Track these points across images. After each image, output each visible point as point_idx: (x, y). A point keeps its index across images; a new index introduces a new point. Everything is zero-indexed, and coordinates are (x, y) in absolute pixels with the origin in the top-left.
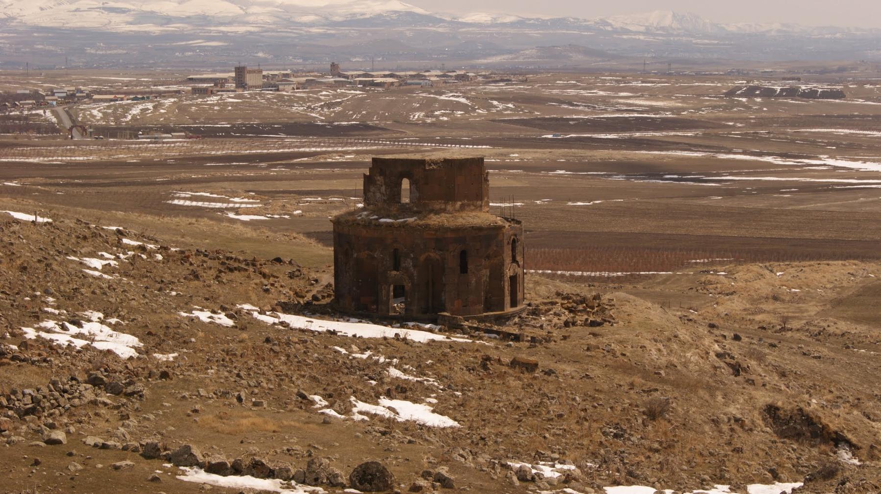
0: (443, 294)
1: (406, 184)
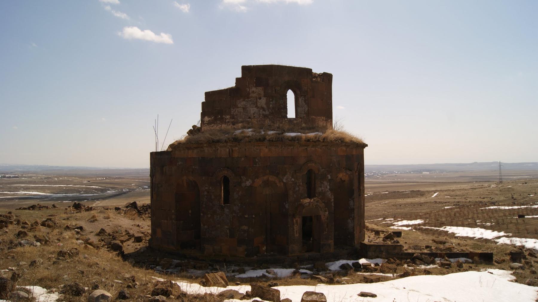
0: (349, 221)
1: (290, 96)
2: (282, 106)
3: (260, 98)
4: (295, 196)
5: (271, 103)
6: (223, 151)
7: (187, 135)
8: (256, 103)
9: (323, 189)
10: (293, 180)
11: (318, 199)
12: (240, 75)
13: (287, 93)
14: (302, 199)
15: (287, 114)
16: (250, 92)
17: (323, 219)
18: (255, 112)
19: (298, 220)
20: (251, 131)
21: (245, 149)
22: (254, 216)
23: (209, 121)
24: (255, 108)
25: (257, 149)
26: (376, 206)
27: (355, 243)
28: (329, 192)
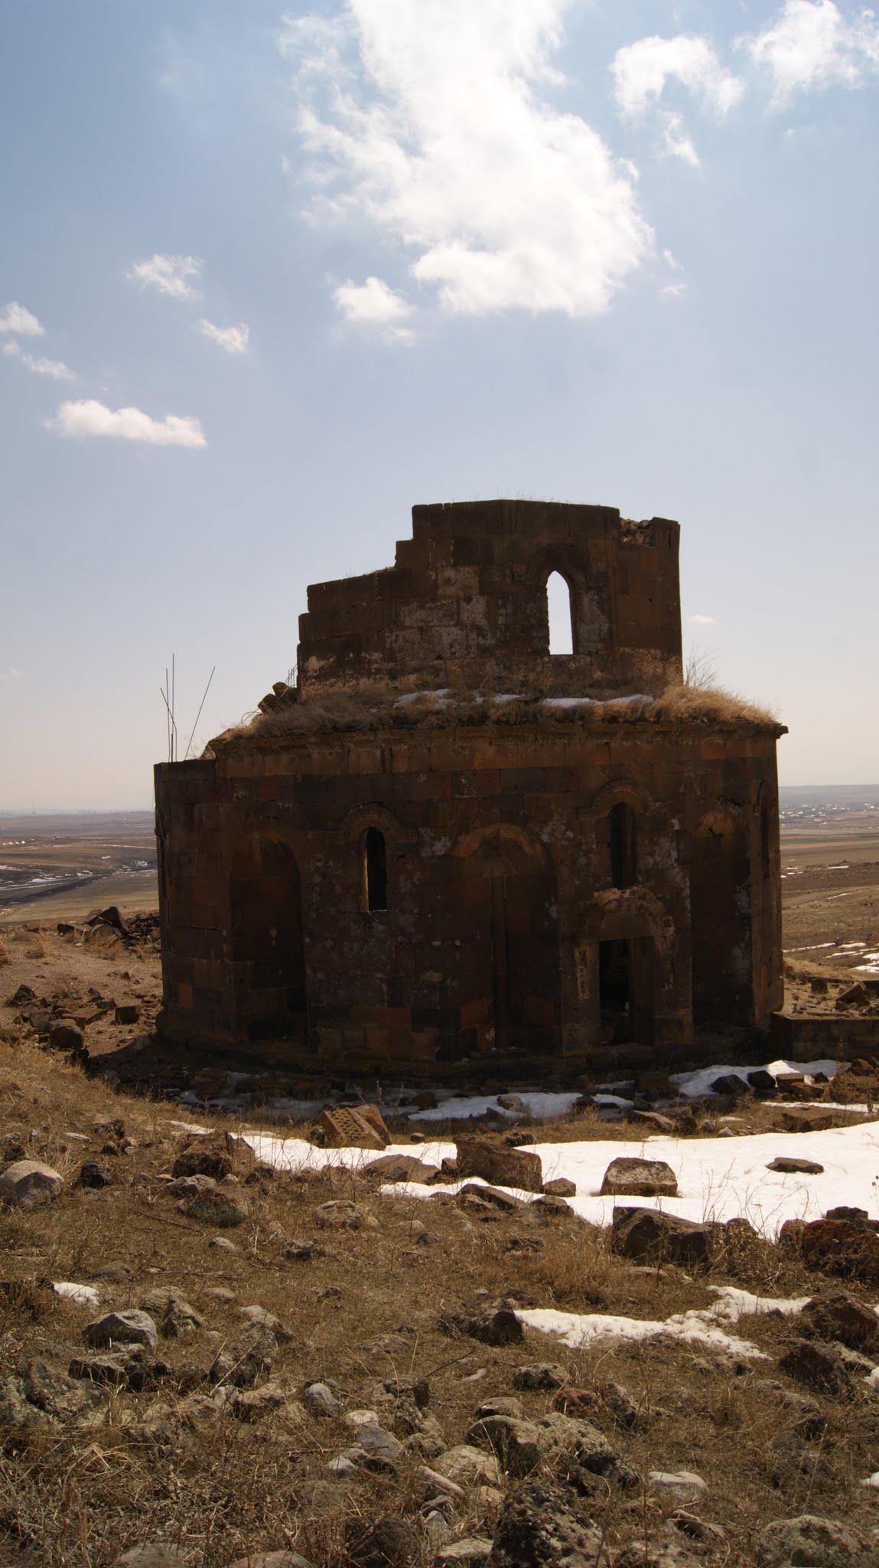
0: (737, 952)
1: (557, 588)
2: (533, 621)
3: (469, 600)
4: (577, 882)
5: (502, 611)
6: (364, 757)
7: (260, 711)
8: (459, 614)
9: (658, 859)
10: (570, 834)
11: (643, 890)
12: (408, 534)
13: (546, 583)
14: (597, 890)
15: (548, 642)
16: (440, 581)
17: (660, 945)
18: (455, 640)
19: (588, 951)
20: (446, 696)
21: (429, 750)
22: (458, 943)
23: (321, 668)
24: (455, 630)
25: (463, 748)
26: (812, 907)
27: (754, 1015)
28: (677, 869)
